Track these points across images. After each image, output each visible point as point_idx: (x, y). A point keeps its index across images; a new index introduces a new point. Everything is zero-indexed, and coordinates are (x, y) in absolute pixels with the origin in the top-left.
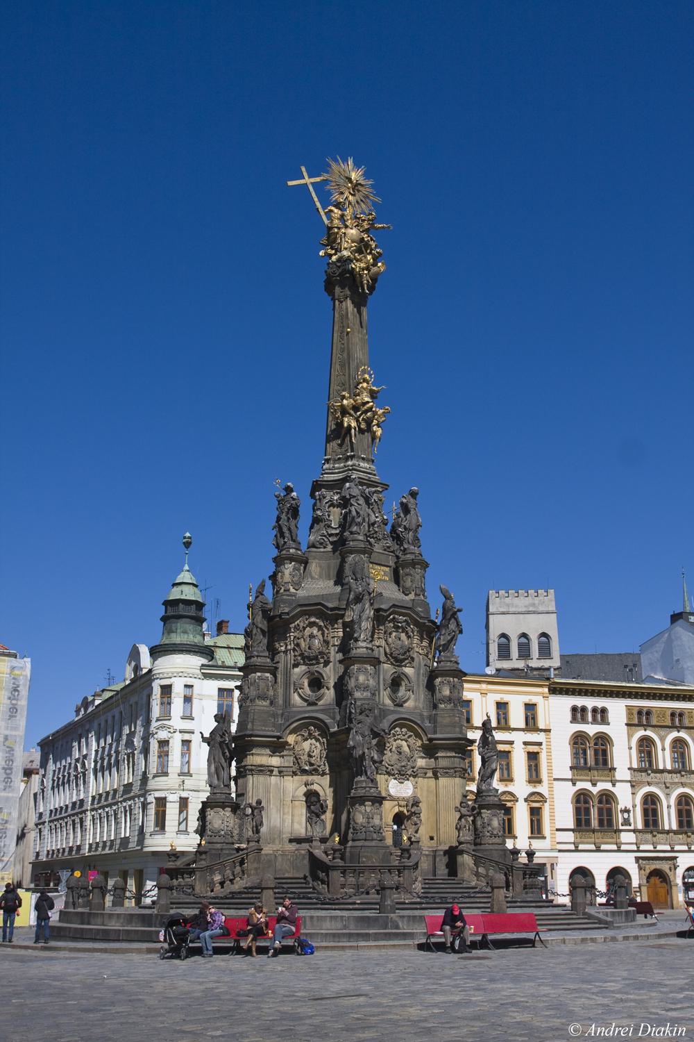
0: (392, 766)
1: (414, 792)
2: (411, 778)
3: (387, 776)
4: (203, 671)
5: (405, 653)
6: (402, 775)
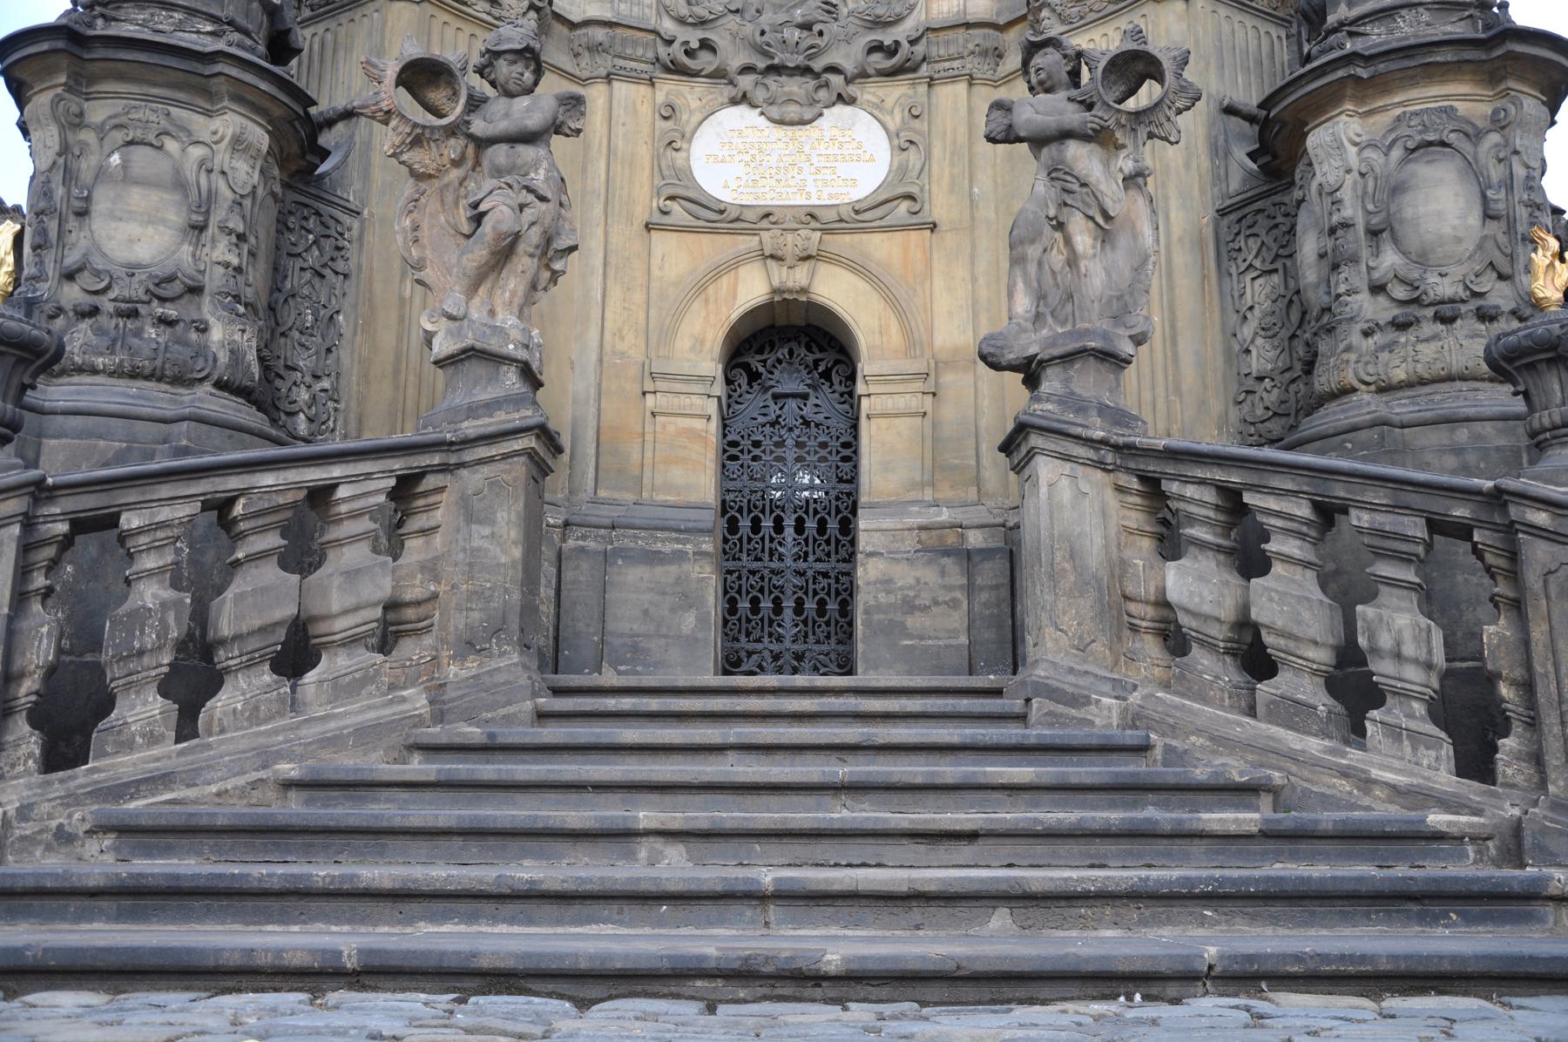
0: (702, 23)
1: (899, 172)
2: (869, 92)
3: (669, 88)
6: (792, 76)
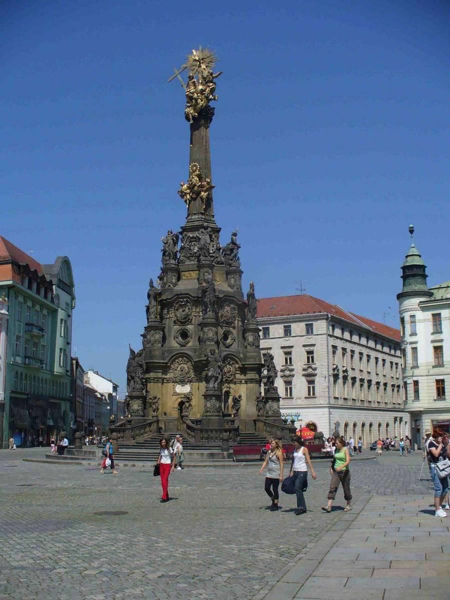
1: (191, 390)
3: (173, 384)
4: (420, 306)
5: (185, 318)
6: (182, 382)
